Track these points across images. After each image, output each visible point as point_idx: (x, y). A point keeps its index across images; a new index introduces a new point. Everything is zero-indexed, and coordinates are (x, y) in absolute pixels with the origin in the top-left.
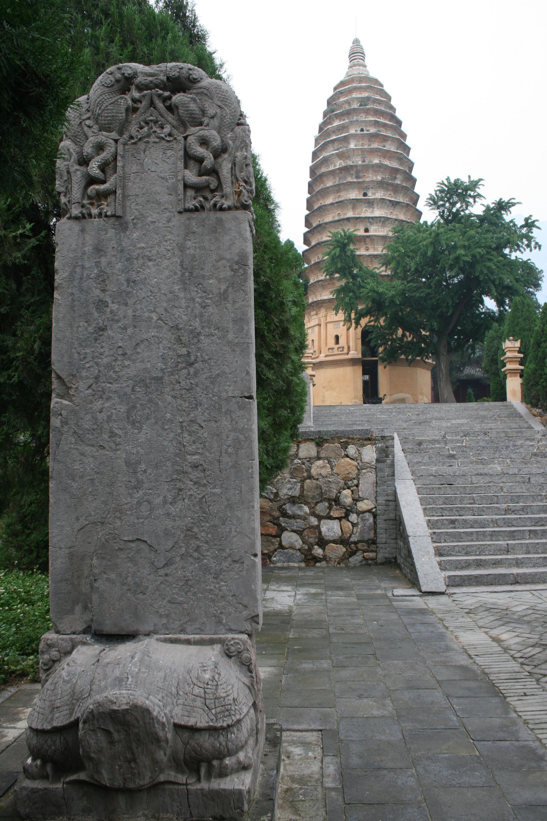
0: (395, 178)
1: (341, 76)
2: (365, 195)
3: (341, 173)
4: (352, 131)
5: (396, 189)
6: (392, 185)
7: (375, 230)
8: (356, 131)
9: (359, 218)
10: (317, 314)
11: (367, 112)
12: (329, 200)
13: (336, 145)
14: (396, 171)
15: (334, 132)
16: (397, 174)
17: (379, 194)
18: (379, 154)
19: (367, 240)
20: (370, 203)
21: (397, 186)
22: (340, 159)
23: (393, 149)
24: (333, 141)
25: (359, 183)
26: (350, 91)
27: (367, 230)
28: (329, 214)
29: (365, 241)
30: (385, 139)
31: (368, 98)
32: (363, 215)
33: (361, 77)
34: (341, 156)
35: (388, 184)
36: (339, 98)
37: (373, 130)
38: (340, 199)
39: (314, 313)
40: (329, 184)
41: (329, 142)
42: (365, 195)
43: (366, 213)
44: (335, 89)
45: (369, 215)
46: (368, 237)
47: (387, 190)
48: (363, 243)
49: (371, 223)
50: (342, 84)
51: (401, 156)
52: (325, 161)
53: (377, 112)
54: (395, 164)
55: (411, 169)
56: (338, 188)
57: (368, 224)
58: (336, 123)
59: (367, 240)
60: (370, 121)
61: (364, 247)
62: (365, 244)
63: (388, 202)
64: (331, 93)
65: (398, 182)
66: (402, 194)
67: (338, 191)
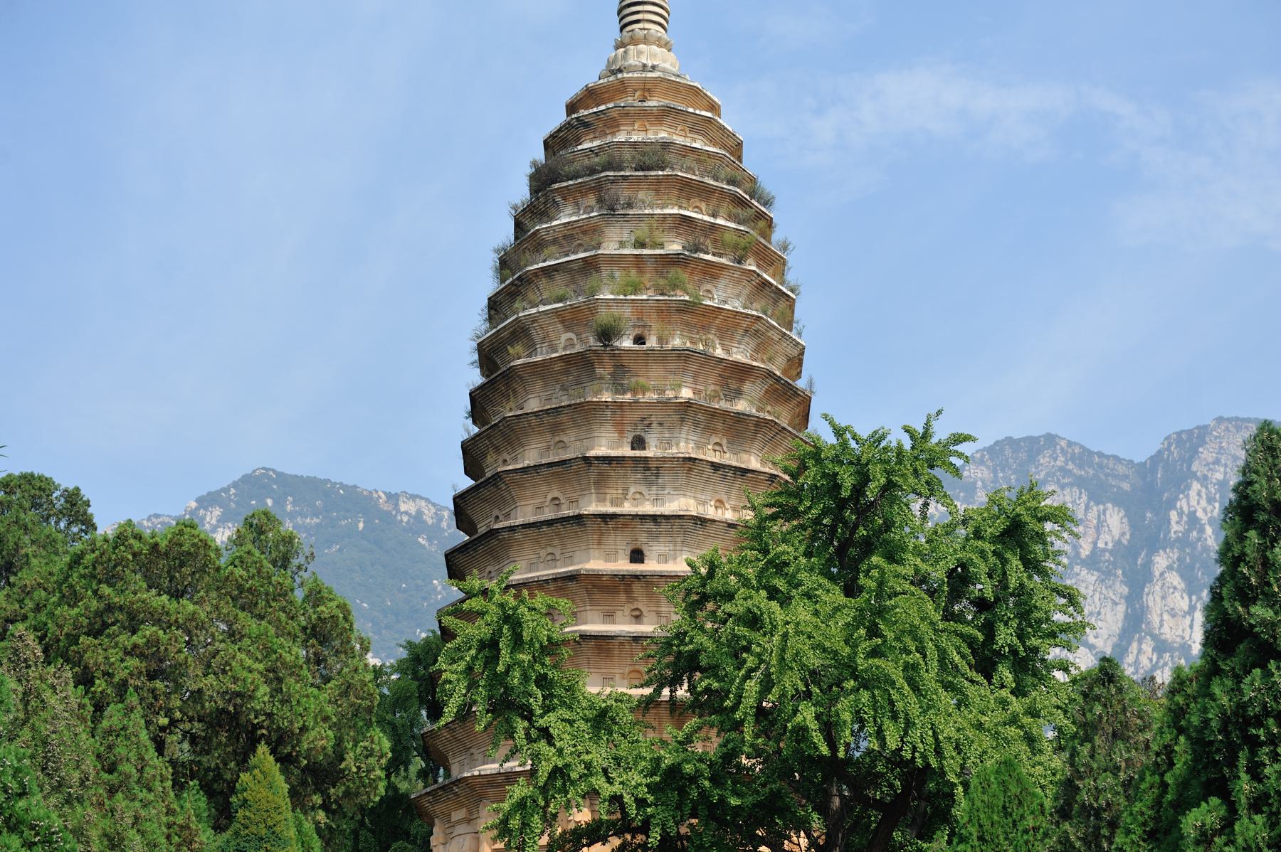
0: (738, 394)
1: (590, 74)
2: (639, 443)
3: (567, 372)
4: (610, 248)
5: (739, 428)
6: (725, 414)
7: (663, 558)
8: (622, 245)
9: (614, 516)
10: (469, 821)
11: (658, 186)
12: (530, 457)
13: (559, 285)
14: (742, 371)
15: (555, 241)
16: (742, 381)
17: (685, 446)
18: (688, 318)
19: (637, 587)
20: (648, 470)
21: (740, 417)
22: (568, 328)
23: (735, 305)
24: (548, 272)
25: (621, 406)
26: (612, 124)
27: (637, 556)
28: (525, 498)
29: (629, 592)
30: (712, 272)
31: (666, 146)
32: (627, 508)
33: (645, 81)
34: (570, 319)
35: (714, 414)
36: (578, 141)
37: (674, 247)
38: (564, 457)
39: (457, 815)
40: (533, 405)
41: (536, 273)
42: (639, 443)
43: (638, 501)
44: (571, 108)
45: (648, 508)
46: (636, 577)
47: (710, 430)
48: (623, 597)
49: (654, 536)
50: (590, 95)
51: (757, 327)
52: (520, 333)
53: (688, 190)
54: (740, 355)
55: (796, 363)
56: (552, 420)
57: (643, 538)
58: (566, 217)
59: (637, 587)
60: (665, 217)
61: (627, 609)
62: (630, 598)
63: (708, 470)
64: (561, 117)
65: (741, 406)
66: (757, 444)
67: (556, 429)
